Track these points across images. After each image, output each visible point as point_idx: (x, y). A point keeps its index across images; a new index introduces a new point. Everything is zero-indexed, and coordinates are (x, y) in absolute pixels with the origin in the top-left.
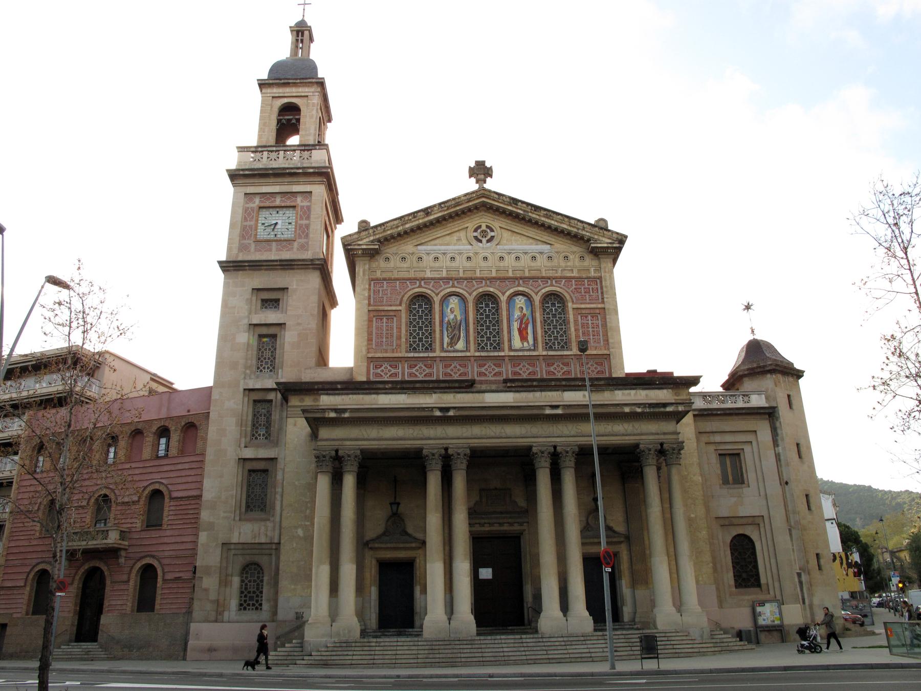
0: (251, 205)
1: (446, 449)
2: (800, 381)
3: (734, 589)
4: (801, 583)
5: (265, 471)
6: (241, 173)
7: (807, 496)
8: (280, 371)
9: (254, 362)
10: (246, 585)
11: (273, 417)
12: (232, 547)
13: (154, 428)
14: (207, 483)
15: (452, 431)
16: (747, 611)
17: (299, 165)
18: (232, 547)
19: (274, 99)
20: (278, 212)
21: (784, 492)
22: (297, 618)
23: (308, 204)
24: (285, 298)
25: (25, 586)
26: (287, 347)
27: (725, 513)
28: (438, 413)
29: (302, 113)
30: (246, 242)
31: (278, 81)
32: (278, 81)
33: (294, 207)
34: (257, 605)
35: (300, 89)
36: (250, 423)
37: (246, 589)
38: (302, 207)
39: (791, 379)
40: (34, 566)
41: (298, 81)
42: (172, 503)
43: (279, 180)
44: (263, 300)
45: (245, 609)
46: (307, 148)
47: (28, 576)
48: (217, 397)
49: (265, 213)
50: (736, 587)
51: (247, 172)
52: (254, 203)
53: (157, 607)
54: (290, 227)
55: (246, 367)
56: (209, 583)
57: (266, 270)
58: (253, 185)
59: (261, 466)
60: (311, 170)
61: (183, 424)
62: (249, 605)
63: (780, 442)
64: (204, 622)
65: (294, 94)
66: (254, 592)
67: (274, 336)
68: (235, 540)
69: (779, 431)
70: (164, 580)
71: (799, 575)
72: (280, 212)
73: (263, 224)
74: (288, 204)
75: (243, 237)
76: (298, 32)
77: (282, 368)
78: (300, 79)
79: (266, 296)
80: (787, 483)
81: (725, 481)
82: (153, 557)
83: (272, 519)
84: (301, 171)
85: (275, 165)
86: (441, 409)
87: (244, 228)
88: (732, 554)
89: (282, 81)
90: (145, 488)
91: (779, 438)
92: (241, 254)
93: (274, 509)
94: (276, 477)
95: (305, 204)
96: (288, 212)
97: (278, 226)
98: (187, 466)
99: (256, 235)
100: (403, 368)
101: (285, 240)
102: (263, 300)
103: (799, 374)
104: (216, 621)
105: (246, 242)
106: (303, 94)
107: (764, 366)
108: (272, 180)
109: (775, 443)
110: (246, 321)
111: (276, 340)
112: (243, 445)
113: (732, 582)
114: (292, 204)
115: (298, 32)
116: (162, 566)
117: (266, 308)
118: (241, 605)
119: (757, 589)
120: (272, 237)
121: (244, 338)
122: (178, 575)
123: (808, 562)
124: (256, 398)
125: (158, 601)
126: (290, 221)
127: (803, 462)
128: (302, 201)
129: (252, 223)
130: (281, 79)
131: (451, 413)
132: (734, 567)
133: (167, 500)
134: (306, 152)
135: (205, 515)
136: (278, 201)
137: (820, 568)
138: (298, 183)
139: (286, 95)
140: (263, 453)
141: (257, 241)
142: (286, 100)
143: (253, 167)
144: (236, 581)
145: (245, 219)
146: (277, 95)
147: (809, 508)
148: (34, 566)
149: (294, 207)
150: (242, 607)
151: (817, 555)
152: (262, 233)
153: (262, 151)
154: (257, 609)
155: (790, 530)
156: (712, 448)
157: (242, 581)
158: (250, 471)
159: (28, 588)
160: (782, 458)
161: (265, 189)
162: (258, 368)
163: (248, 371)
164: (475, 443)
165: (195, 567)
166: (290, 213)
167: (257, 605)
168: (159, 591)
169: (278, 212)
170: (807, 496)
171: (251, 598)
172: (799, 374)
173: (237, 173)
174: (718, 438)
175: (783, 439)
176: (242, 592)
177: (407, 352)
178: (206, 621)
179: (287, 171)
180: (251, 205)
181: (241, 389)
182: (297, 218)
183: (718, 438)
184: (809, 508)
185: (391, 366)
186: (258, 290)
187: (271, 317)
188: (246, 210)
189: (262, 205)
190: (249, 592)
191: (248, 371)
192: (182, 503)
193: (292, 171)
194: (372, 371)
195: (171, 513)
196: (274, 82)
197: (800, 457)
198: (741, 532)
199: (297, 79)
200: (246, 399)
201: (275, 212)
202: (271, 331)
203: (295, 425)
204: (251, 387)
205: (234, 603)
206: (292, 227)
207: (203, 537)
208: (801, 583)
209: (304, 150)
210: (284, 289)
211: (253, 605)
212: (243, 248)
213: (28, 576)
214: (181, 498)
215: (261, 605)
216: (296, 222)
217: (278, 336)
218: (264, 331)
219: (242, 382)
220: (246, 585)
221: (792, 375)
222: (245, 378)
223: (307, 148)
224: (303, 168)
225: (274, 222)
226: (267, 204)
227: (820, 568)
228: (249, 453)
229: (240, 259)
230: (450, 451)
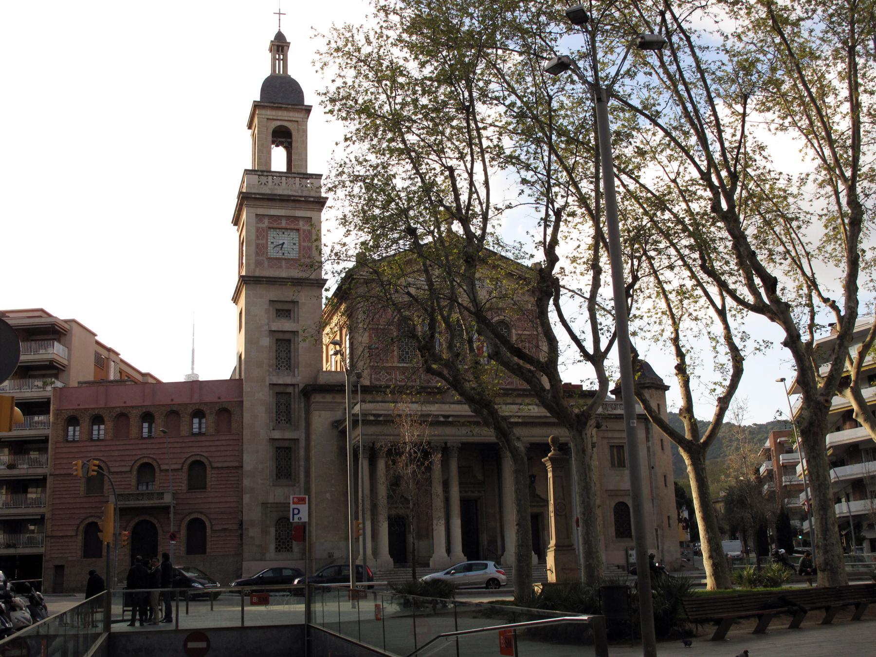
0: (260, 225)
1: (446, 443)
2: (666, 392)
3: (614, 539)
4: (657, 535)
5: (288, 449)
6: (253, 196)
7: (665, 476)
8: (296, 370)
9: (275, 361)
10: (279, 533)
11: (292, 407)
12: (269, 505)
13: (190, 411)
14: (247, 458)
15: (448, 430)
16: (623, 553)
17: (300, 194)
18: (269, 505)
19: (269, 121)
20: (283, 233)
21: (650, 474)
22: (330, 557)
23: (309, 228)
24: (296, 309)
25: (77, 535)
26: (301, 352)
27: (611, 487)
28: (442, 419)
29: (294, 138)
30: (261, 258)
31: (272, 105)
32: (272, 105)
33: (298, 230)
34: (288, 548)
35: (291, 114)
36: (275, 411)
37: (279, 536)
38: (304, 231)
39: (661, 392)
40: (84, 520)
41: (290, 106)
42: (213, 472)
43: (284, 204)
44: (277, 310)
45: (279, 551)
46: (305, 176)
47: (78, 528)
48: (249, 390)
49: (272, 234)
50: (616, 537)
51: (258, 196)
52: (264, 223)
53: (208, 550)
54: (294, 247)
55: (270, 366)
56: (253, 532)
57: (280, 285)
58: (262, 207)
59: (286, 444)
60: (312, 199)
61: (217, 408)
62: (282, 548)
63: (650, 439)
64: (252, 560)
65: (286, 118)
66: (286, 539)
67: (289, 341)
68: (271, 500)
69: (651, 432)
70: (213, 531)
71: (657, 530)
72: (286, 233)
73: (272, 243)
74: (292, 226)
75: (257, 254)
76: (278, 46)
77: (298, 368)
78: (292, 105)
79: (279, 306)
80: (653, 468)
81: (613, 465)
82: (201, 513)
83: (297, 485)
84: (303, 199)
85: (279, 191)
86: (445, 416)
87: (257, 245)
88: (615, 515)
89: (276, 105)
90: (187, 459)
91: (650, 436)
92: (257, 270)
93: (299, 477)
94: (299, 453)
95: (307, 228)
96: (291, 234)
97: (285, 246)
98: (224, 443)
99: (267, 253)
100: (396, 375)
101: (293, 259)
102: (277, 310)
103: (667, 388)
104: (261, 560)
105: (261, 258)
106: (294, 119)
107: (644, 384)
108: (278, 204)
109: (648, 439)
110: (266, 328)
111: (290, 344)
112: (271, 428)
113: (614, 534)
114: (296, 227)
115: (278, 46)
116: (210, 520)
117: (279, 316)
118: (276, 548)
119: (629, 539)
120: (280, 255)
121: (266, 341)
122: (225, 527)
123: (662, 522)
124: (278, 391)
125: (208, 546)
126: (294, 242)
127: (664, 453)
128: (303, 226)
129: (264, 242)
130: (275, 103)
131: (450, 419)
132: (615, 524)
133: (208, 468)
134: (304, 180)
135: (246, 482)
136: (284, 224)
137: (669, 526)
138: (300, 209)
139: (279, 118)
140: (289, 435)
141: (270, 259)
142: (279, 123)
143: (260, 192)
144: (273, 530)
145: (257, 238)
146: (271, 117)
147: (666, 486)
148: (84, 520)
149: (298, 230)
150: (278, 549)
151: (669, 517)
152: (273, 253)
153: (267, 176)
154: (288, 551)
155: (653, 500)
156: (605, 441)
157: (276, 531)
158: (277, 448)
159: (80, 538)
160: (651, 450)
161: (273, 212)
162: (277, 366)
163: (271, 369)
164: (465, 439)
165: (242, 521)
166: (294, 235)
167: (288, 548)
168: (208, 539)
169: (283, 233)
170: (665, 476)
171: (284, 543)
172: (667, 388)
173: (249, 196)
174: (610, 435)
175: (652, 437)
176: (276, 539)
177: (399, 362)
178: (254, 560)
179: (292, 198)
180: (260, 225)
181: (267, 384)
182: (299, 240)
183: (610, 435)
184: (666, 486)
185: (387, 373)
186: (273, 301)
187: (286, 325)
188: (258, 229)
189: (271, 225)
190: (282, 539)
191: (271, 369)
192: (222, 471)
193: (296, 198)
194: (373, 376)
195: (213, 479)
196: (269, 104)
197: (663, 449)
198: (621, 500)
199: (289, 105)
200: (271, 392)
201: (281, 233)
202: (287, 336)
203: (320, 416)
204: (275, 382)
205: (272, 547)
206: (296, 247)
207: (246, 498)
208: (657, 535)
209: (303, 178)
210: (295, 303)
211: (286, 548)
212: (259, 264)
213: (78, 528)
214: (222, 468)
215: (291, 548)
216: (300, 243)
217: (292, 341)
218: (281, 336)
219: (267, 378)
220: (279, 533)
221: (662, 389)
222: (269, 375)
223: (305, 176)
224: (305, 197)
225: (281, 242)
226: (275, 225)
227: (669, 526)
228: (277, 435)
229: (257, 274)
230: (449, 445)
